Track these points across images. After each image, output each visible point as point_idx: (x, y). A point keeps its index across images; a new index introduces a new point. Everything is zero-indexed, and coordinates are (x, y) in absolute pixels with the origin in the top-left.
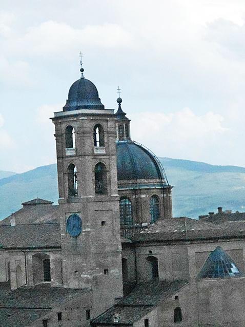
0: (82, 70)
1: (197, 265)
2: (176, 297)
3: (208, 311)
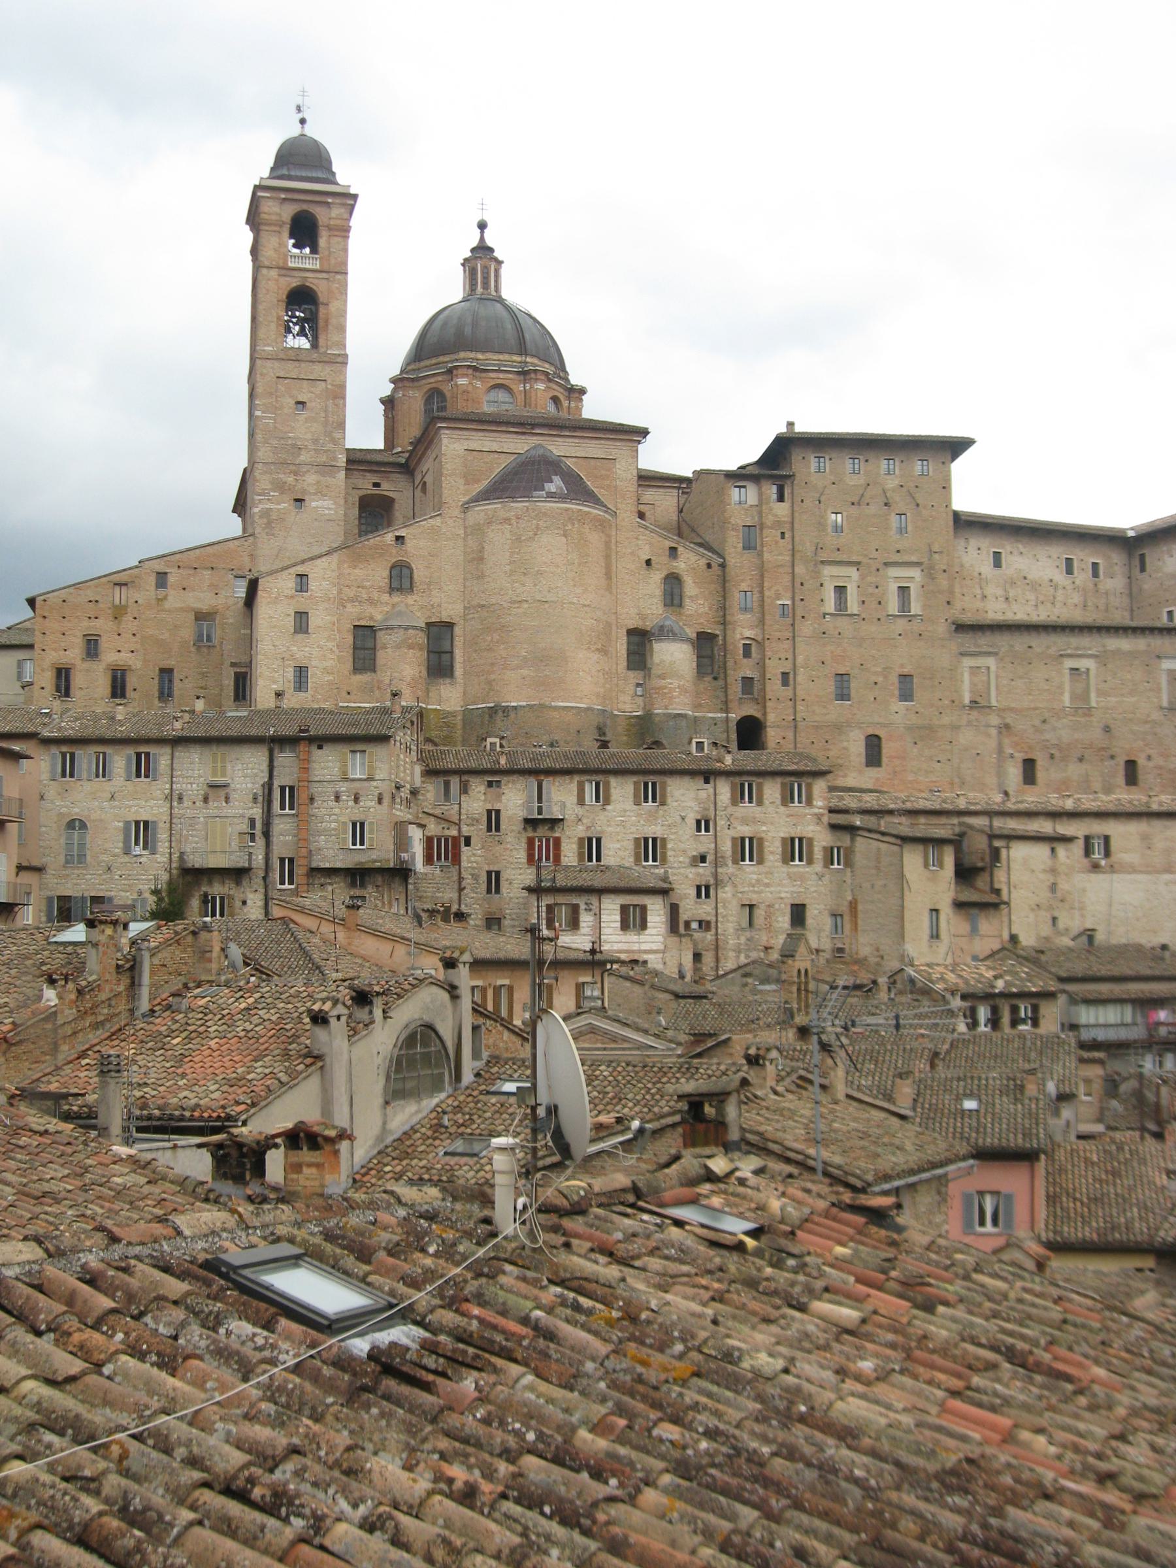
0: (303, 121)
1: (469, 478)
2: (399, 539)
3: (481, 577)
